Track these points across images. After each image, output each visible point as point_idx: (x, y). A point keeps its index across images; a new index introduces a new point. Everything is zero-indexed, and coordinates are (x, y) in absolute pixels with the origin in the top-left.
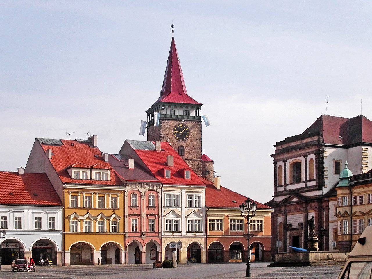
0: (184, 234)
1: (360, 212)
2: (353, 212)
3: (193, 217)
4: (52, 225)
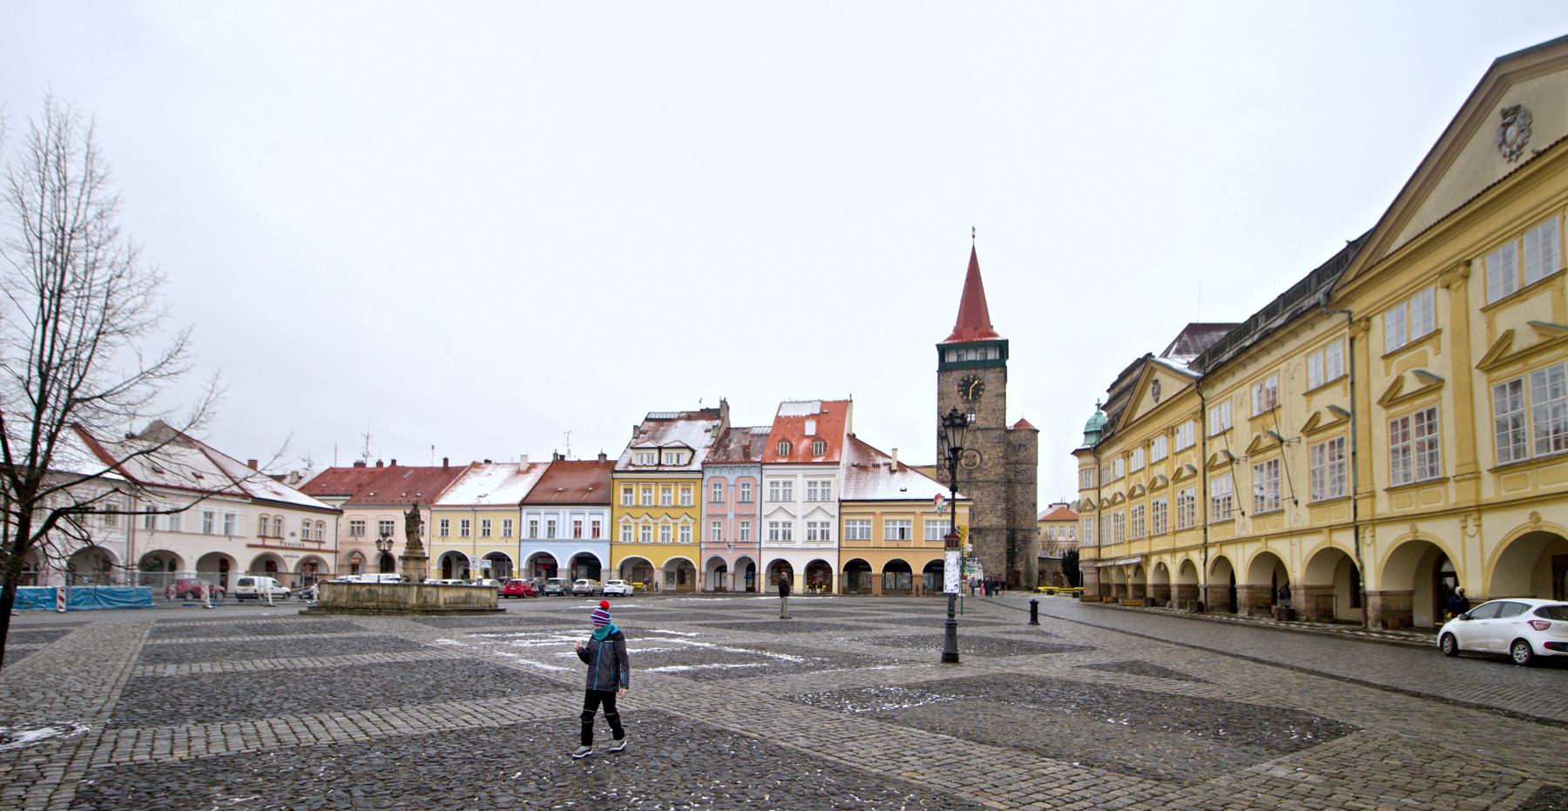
0: (798, 545)
3: (819, 518)
4: (596, 532)
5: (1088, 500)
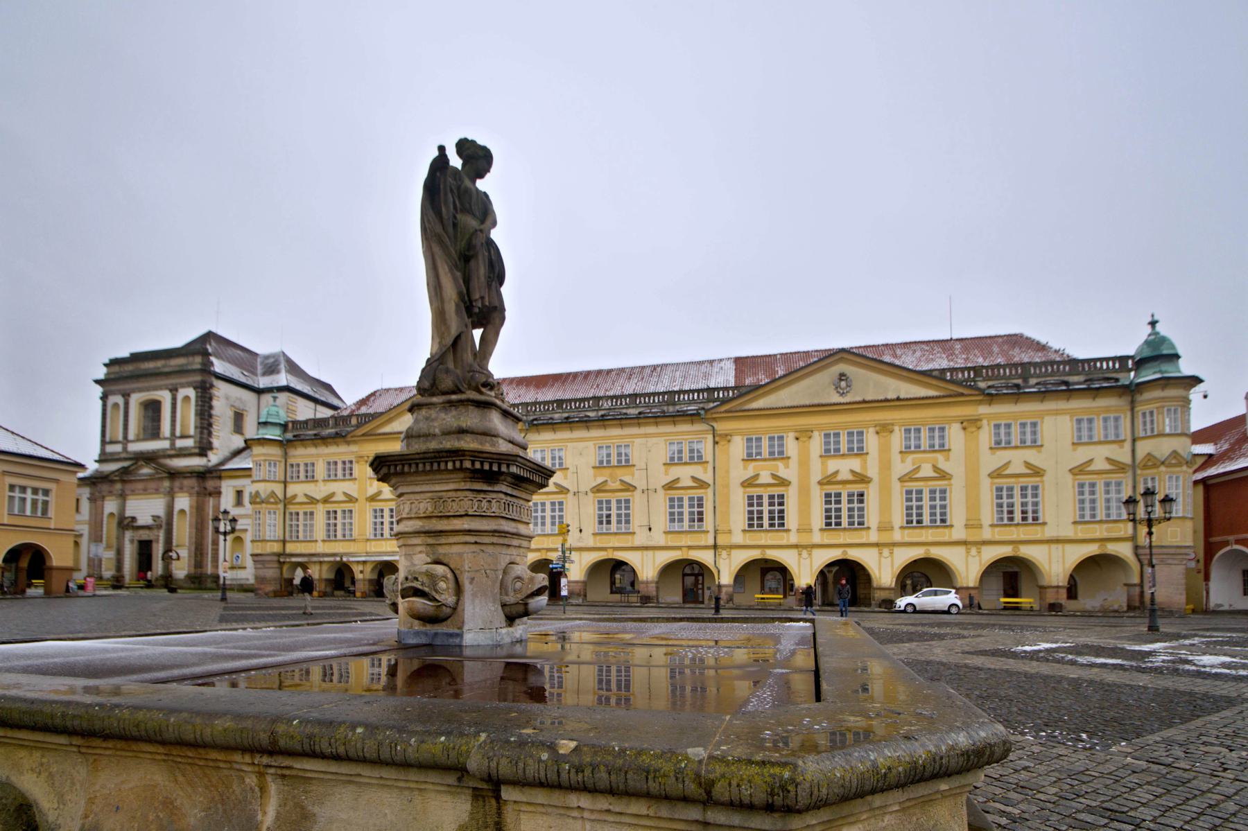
1: (306, 495)
2: (289, 494)
5: (273, 492)
